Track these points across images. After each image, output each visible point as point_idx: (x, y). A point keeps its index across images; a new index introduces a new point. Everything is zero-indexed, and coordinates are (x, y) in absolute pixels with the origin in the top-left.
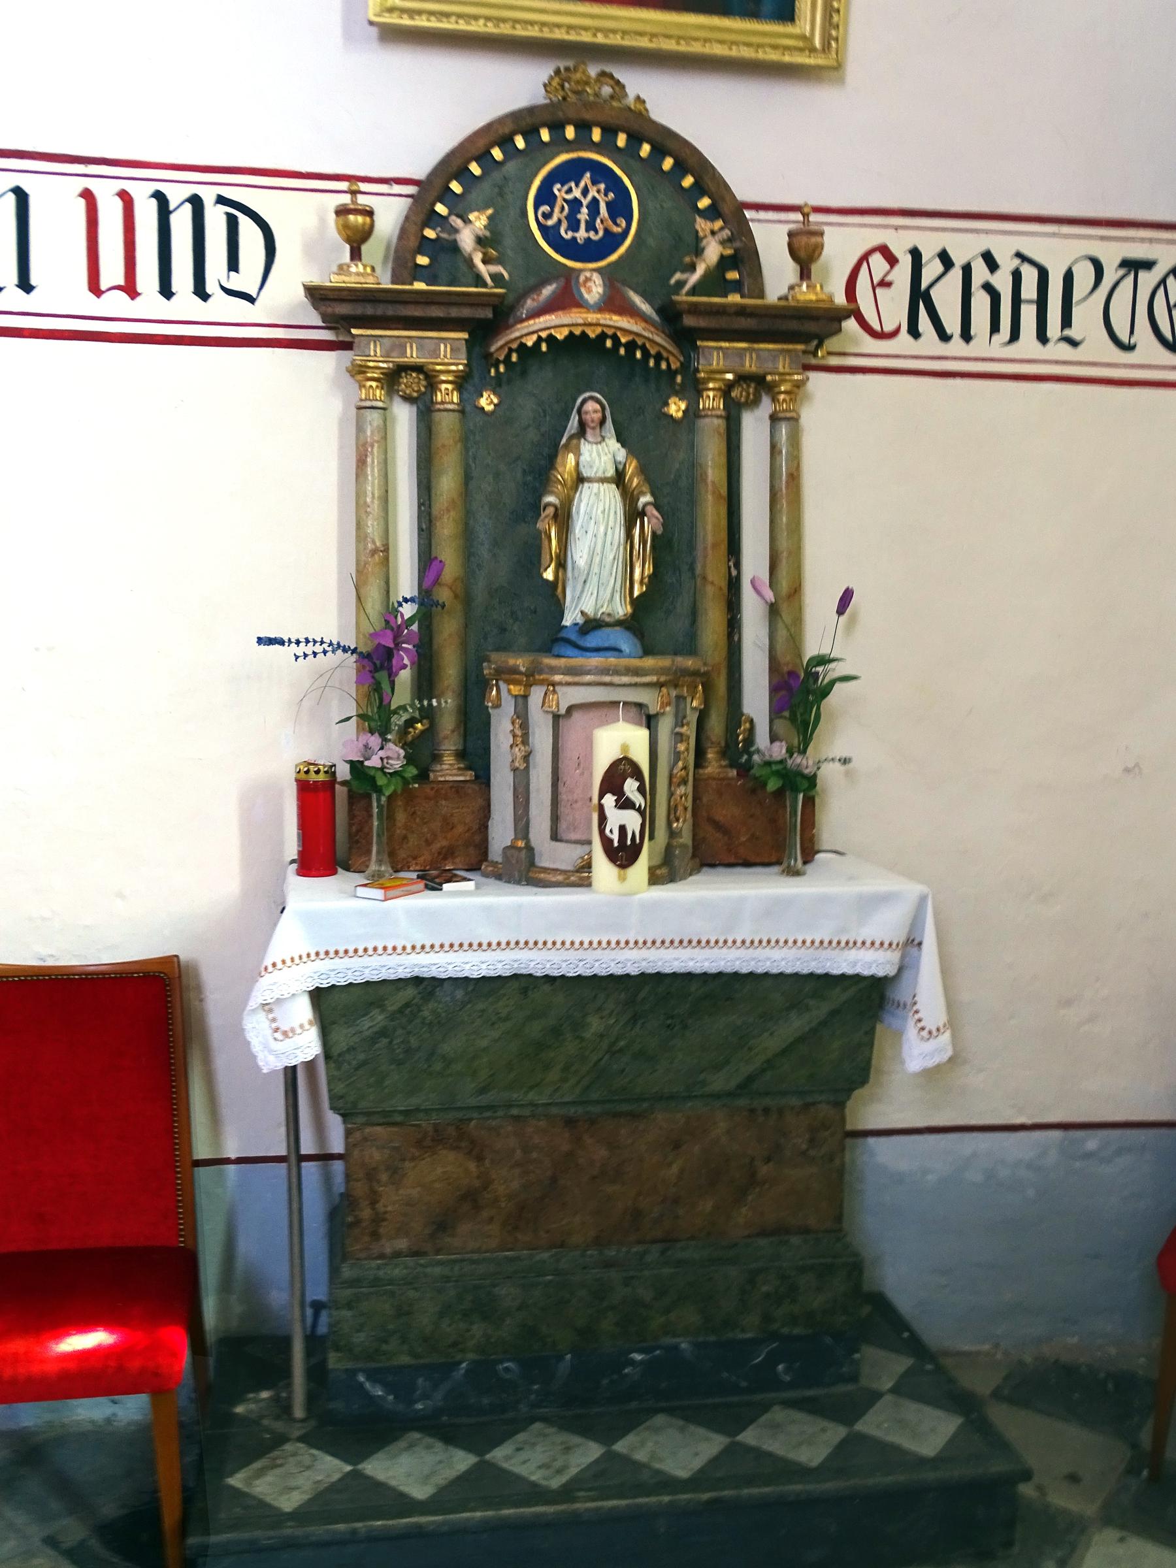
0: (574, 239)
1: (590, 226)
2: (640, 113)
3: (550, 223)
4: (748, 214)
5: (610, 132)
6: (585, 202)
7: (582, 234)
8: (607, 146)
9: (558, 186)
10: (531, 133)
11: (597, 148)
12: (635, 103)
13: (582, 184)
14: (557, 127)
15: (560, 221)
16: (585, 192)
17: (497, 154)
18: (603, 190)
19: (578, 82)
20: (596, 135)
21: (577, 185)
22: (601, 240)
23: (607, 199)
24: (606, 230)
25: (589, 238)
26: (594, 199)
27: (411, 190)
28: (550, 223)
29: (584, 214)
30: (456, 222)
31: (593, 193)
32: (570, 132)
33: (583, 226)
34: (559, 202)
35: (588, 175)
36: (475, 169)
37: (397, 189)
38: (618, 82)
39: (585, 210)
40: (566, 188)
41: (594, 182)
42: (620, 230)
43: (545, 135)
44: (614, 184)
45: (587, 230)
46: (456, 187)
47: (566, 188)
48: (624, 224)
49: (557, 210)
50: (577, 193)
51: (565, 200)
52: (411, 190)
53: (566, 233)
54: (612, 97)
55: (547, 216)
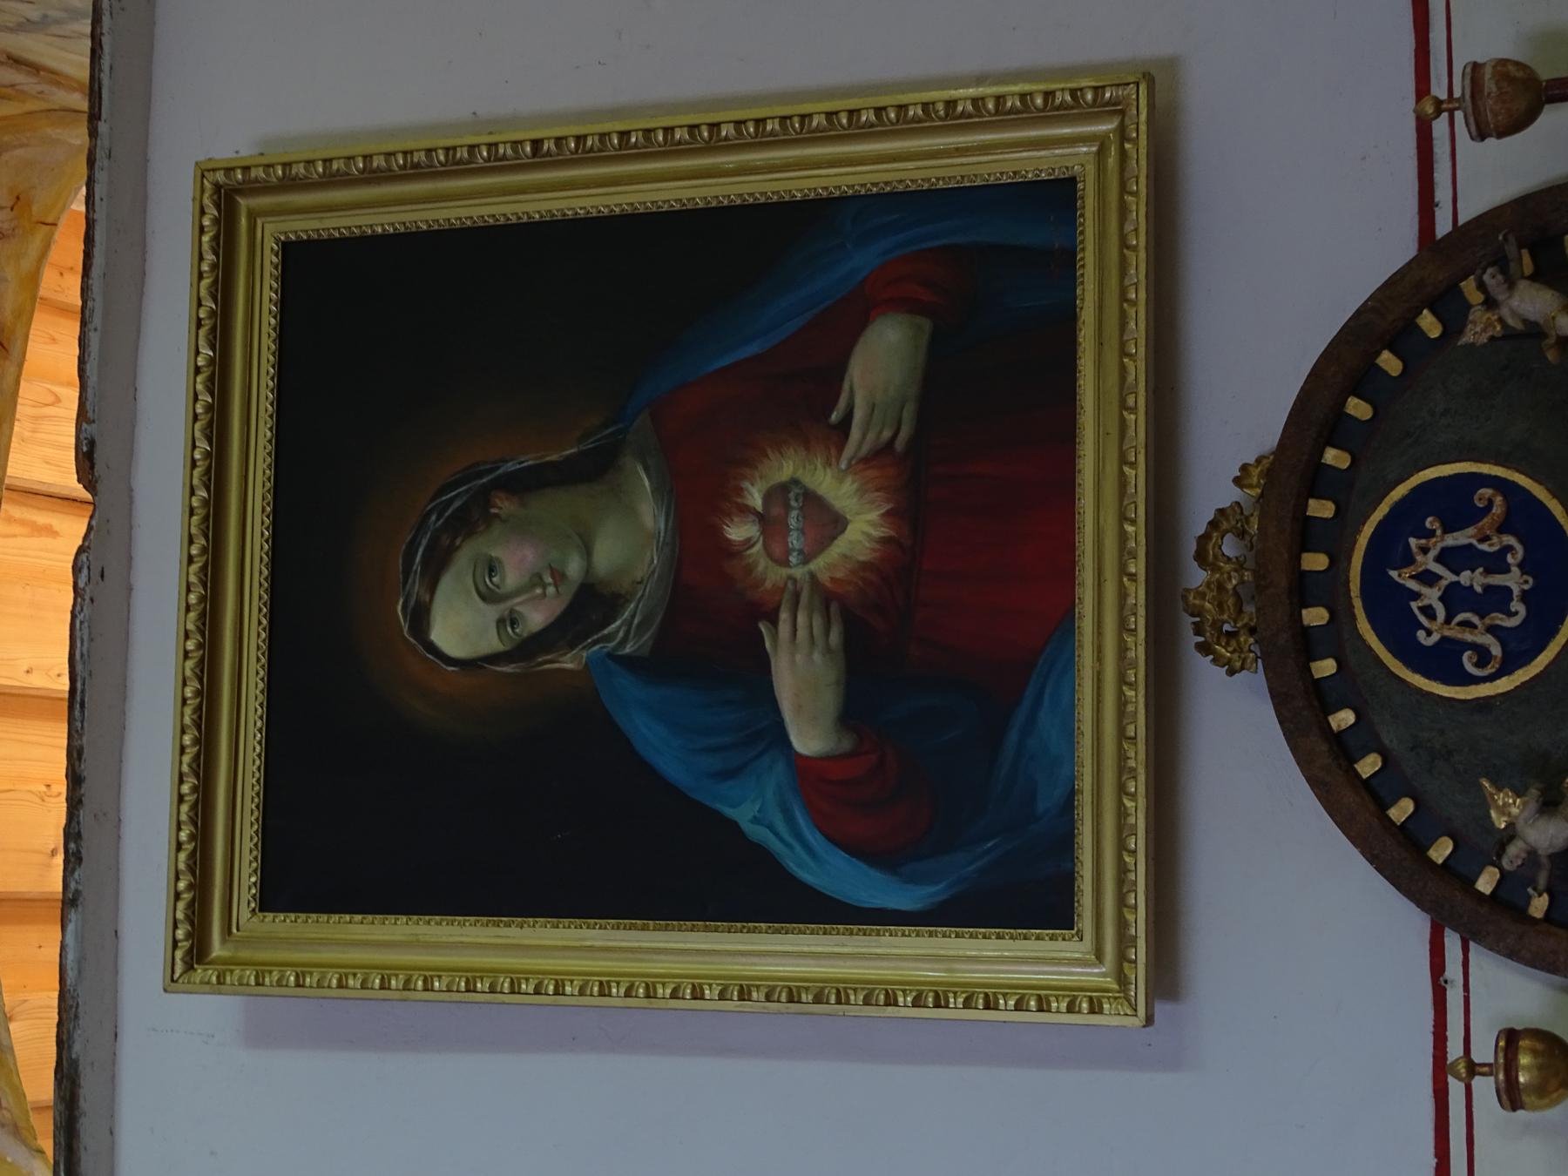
0: (1525, 597)
1: (1496, 563)
2: (1269, 474)
3: (1496, 650)
4: (1443, 227)
5: (1307, 534)
6: (1449, 577)
7: (1514, 581)
8: (1334, 539)
9: (1421, 634)
10: (1323, 698)
11: (1339, 559)
12: (1250, 486)
13: (1413, 585)
14: (1308, 644)
15: (1493, 630)
16: (1428, 578)
17: (1368, 766)
18: (1423, 541)
19: (1221, 606)
20: (1316, 562)
21: (1416, 596)
22: (1534, 578)
23: (1439, 532)
24: (1501, 530)
25: (1521, 566)
26: (1444, 557)
27: (1452, 942)
28: (1496, 650)
29: (1473, 579)
30: (1514, 850)
31: (1429, 563)
32: (1315, 616)
33: (1497, 580)
34: (1453, 632)
35: (1394, 574)
36: (1402, 810)
37: (1453, 970)
38: (1213, 524)
39: (1465, 578)
40: (1422, 619)
41: (1409, 560)
42: (1499, 500)
43: (1325, 668)
44: (1406, 518)
45: (1506, 570)
46: (1441, 851)
47: (1422, 619)
48: (1486, 492)
49: (1468, 637)
50: (1432, 596)
51: (1448, 621)
52: (1452, 942)
53: (1516, 613)
54: (1242, 534)
55: (1483, 656)
